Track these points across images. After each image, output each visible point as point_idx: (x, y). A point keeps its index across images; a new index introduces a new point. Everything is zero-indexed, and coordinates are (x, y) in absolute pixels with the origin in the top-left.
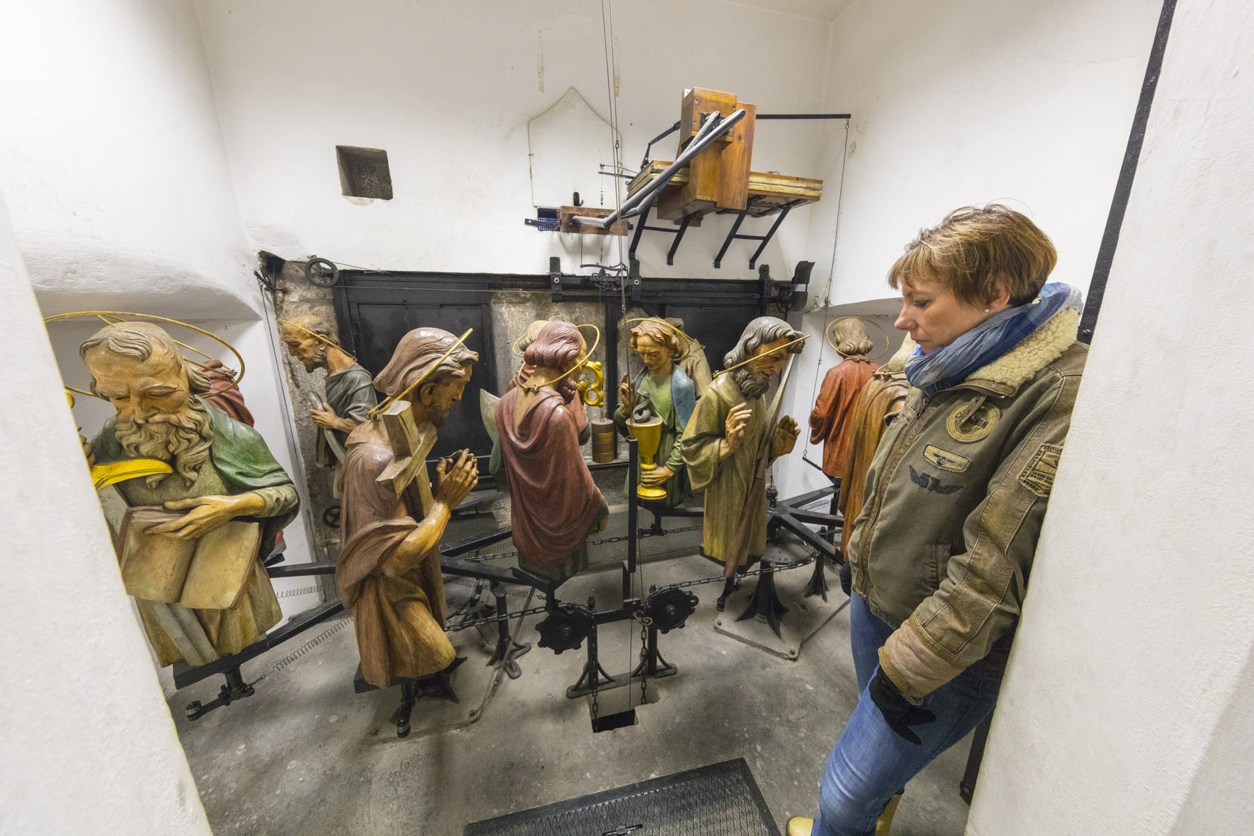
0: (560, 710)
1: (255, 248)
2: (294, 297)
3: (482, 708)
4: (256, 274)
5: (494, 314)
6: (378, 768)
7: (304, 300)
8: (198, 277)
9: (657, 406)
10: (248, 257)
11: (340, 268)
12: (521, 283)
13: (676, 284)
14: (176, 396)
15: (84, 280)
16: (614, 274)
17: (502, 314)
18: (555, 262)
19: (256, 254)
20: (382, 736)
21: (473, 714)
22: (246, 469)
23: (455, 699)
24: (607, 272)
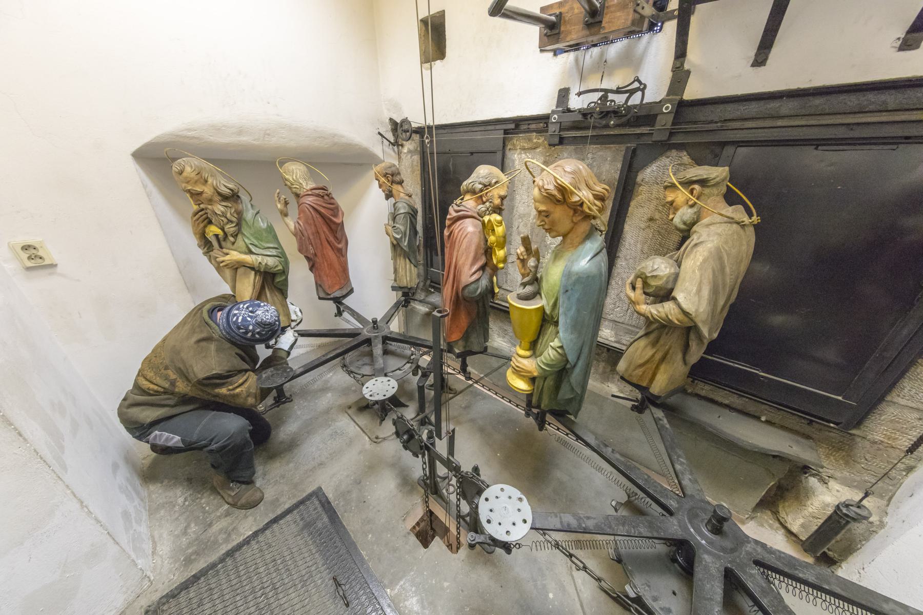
0: (406, 483)
1: (387, 115)
2: (405, 150)
3: (384, 439)
4: (379, 133)
5: (507, 161)
6: (337, 424)
7: (410, 151)
8: (343, 137)
9: (545, 286)
10: (382, 123)
11: (414, 125)
12: (533, 126)
13: (773, 105)
14: (204, 195)
15: (274, 139)
16: (620, 99)
17: (513, 161)
18: (564, 94)
19: (387, 121)
20: (350, 412)
21: (377, 438)
22: (256, 243)
23: (381, 424)
24: (611, 96)
